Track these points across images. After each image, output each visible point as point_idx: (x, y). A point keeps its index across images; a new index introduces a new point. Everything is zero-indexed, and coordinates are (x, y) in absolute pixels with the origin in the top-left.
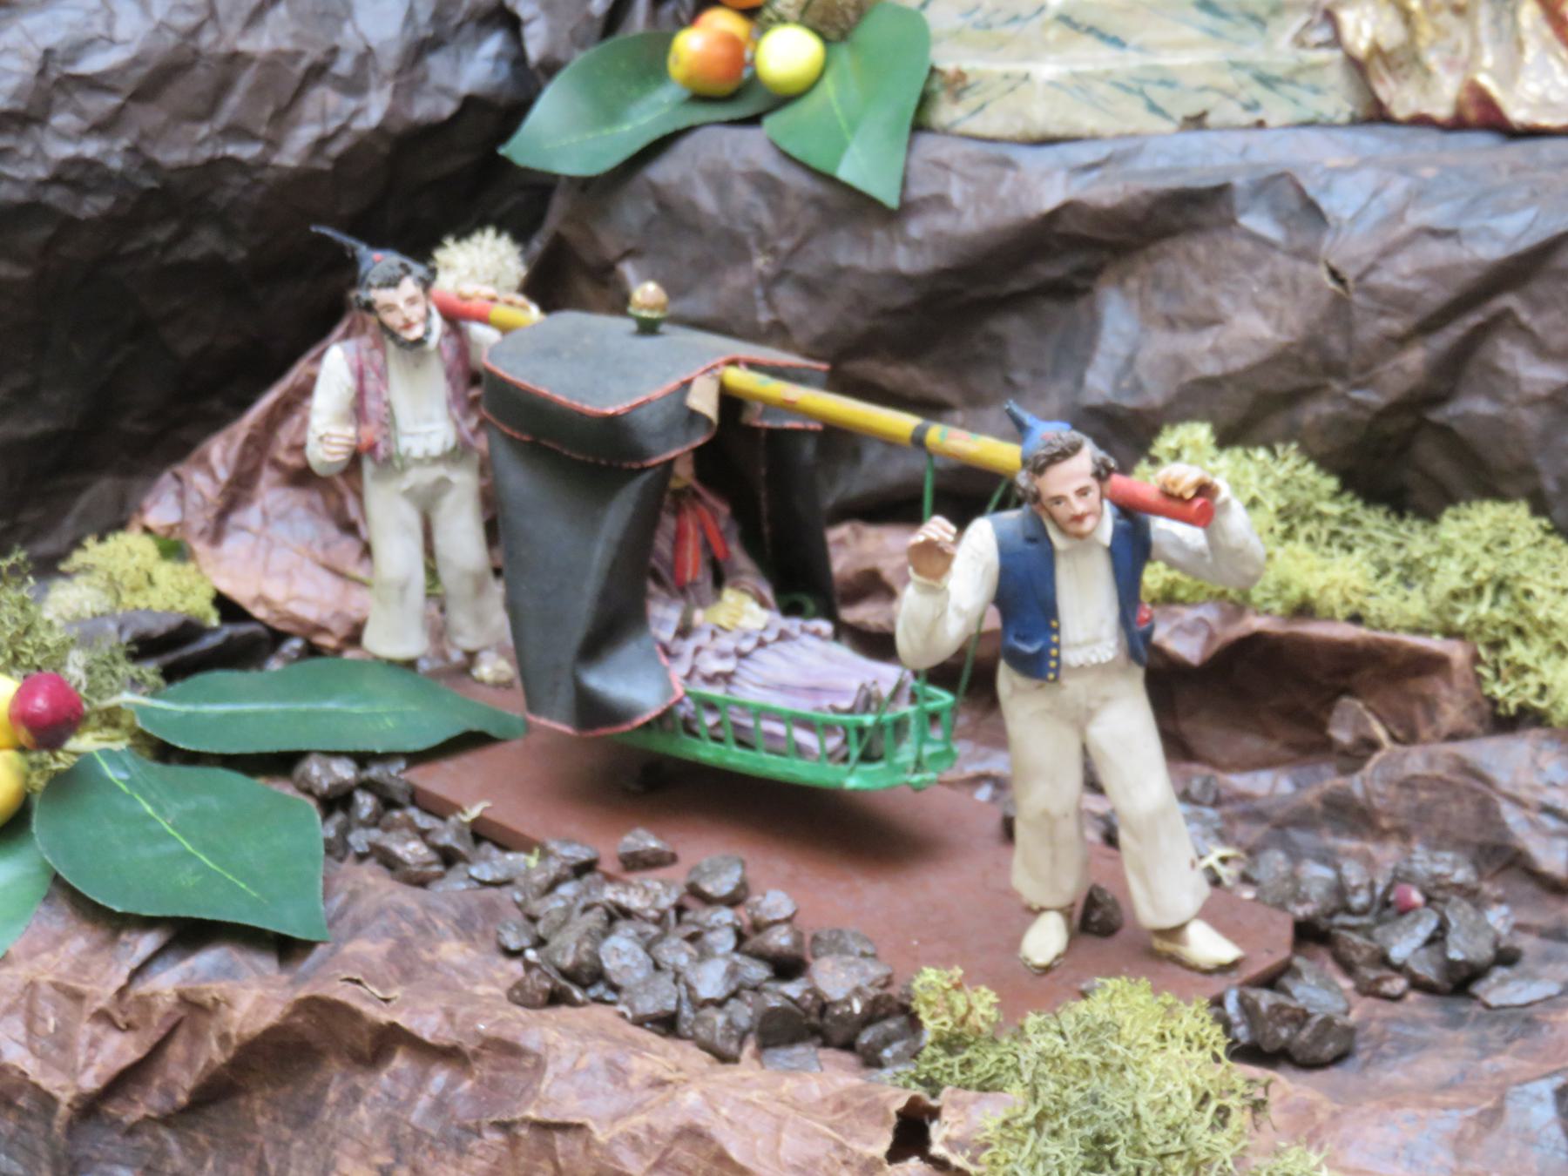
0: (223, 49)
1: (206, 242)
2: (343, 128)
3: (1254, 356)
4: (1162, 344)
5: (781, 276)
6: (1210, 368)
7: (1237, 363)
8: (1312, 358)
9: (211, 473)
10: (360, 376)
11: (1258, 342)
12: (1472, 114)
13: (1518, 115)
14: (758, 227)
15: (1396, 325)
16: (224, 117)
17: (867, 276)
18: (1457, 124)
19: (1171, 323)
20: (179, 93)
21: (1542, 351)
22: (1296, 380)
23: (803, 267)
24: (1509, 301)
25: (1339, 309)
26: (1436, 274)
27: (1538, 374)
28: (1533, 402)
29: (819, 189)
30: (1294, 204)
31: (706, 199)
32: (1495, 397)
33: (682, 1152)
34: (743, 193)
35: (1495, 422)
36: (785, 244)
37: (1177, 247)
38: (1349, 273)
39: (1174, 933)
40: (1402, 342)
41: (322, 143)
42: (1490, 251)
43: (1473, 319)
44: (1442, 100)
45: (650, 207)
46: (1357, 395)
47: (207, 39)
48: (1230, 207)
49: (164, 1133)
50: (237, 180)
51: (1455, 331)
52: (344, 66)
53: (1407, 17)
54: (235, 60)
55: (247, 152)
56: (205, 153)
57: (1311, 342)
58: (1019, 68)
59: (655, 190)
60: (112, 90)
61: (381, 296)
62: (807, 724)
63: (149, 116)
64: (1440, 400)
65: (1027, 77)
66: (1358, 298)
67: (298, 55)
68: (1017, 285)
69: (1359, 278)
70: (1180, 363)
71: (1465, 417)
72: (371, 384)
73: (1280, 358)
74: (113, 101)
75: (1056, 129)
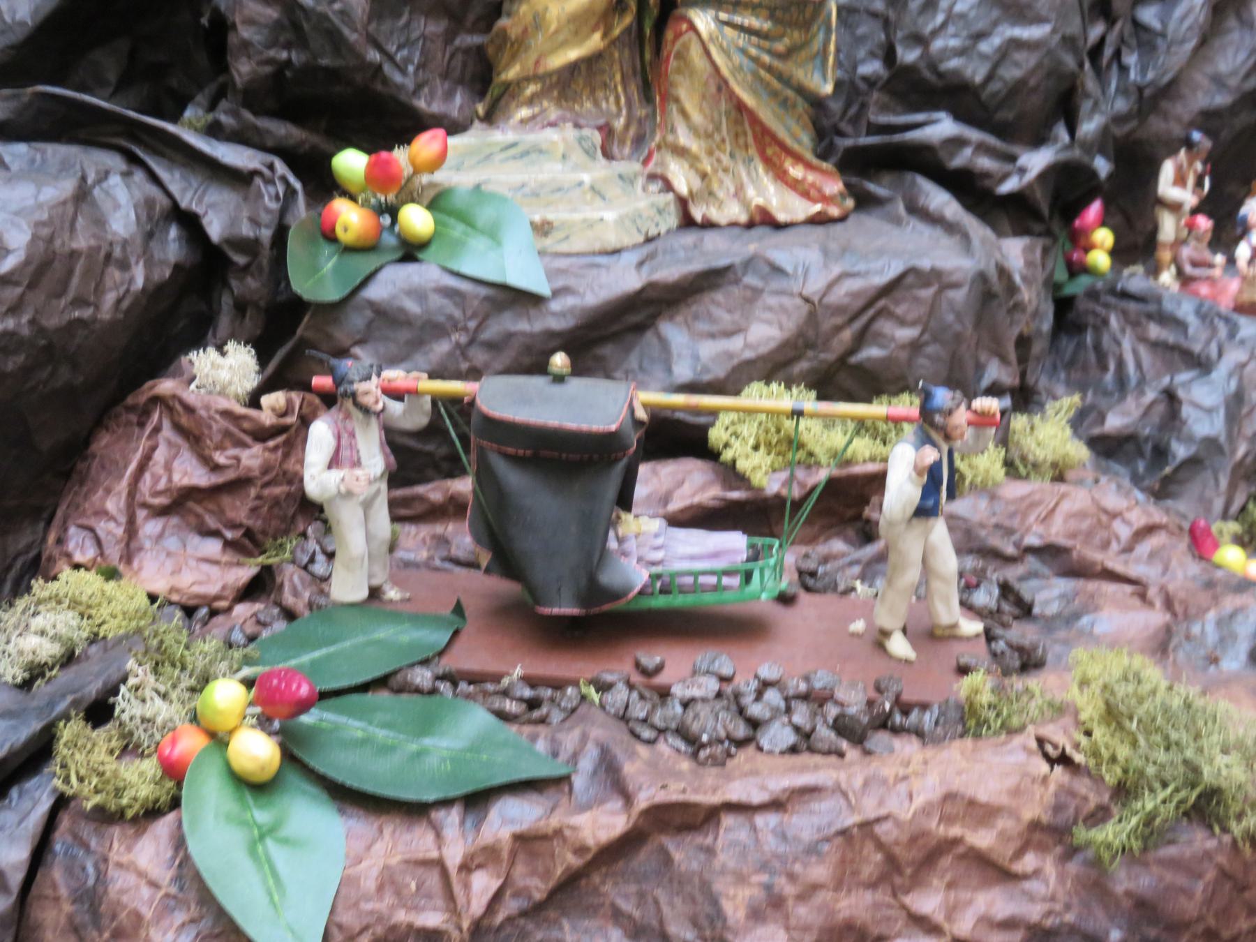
0: (66, 249)
1: (64, 374)
2: (128, 291)
3: (772, 345)
4: (708, 349)
5: (471, 342)
6: (749, 354)
7: (764, 350)
8: (800, 342)
9: (112, 518)
10: (339, 438)
11: (769, 339)
12: (758, 218)
13: (782, 217)
14: (450, 318)
15: (839, 320)
16: (71, 294)
17: (532, 335)
18: (750, 225)
19: (712, 336)
20: (48, 282)
21: (902, 322)
22: (791, 353)
23: (486, 335)
24: (881, 303)
25: (812, 317)
26: (854, 295)
27: (905, 334)
28: (903, 347)
29: (483, 291)
30: (767, 269)
31: (412, 307)
32: (882, 346)
33: (949, 809)
34: (436, 301)
35: (883, 361)
36: (472, 324)
37: (707, 298)
38: (816, 299)
39: (955, 626)
40: (838, 329)
41: (119, 301)
42: (880, 280)
43: (871, 312)
44: (734, 212)
45: (369, 313)
46: (823, 356)
47: (58, 243)
48: (735, 274)
49: (522, 922)
50: (81, 333)
51: (864, 319)
52: (117, 252)
53: (704, 176)
54: (74, 255)
55: (87, 313)
56: (67, 317)
57: (800, 334)
58: (596, 215)
59: (371, 304)
60: (17, 284)
61: (360, 387)
62: (727, 573)
63: (38, 298)
64: (853, 350)
65: (602, 220)
66: (819, 311)
67: (99, 248)
68: (615, 328)
69: (820, 300)
70: (729, 355)
71: (869, 359)
72: (344, 442)
73: (785, 345)
74: (19, 290)
75: (618, 246)
